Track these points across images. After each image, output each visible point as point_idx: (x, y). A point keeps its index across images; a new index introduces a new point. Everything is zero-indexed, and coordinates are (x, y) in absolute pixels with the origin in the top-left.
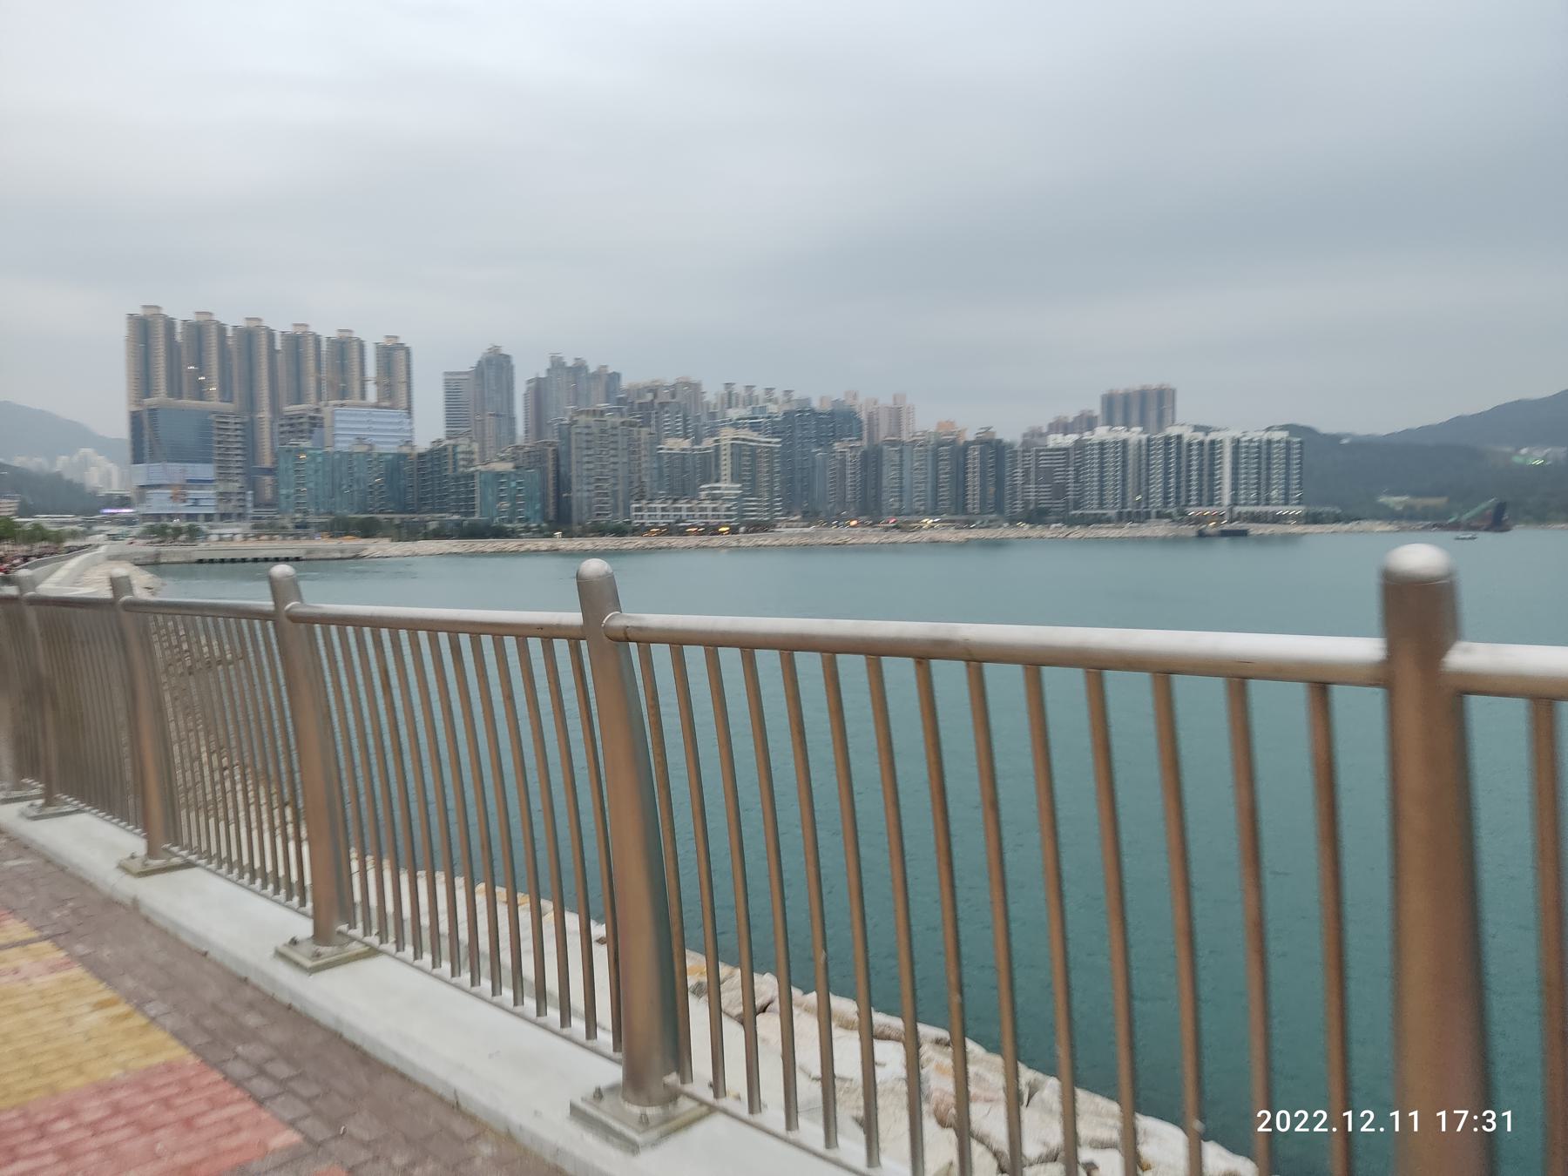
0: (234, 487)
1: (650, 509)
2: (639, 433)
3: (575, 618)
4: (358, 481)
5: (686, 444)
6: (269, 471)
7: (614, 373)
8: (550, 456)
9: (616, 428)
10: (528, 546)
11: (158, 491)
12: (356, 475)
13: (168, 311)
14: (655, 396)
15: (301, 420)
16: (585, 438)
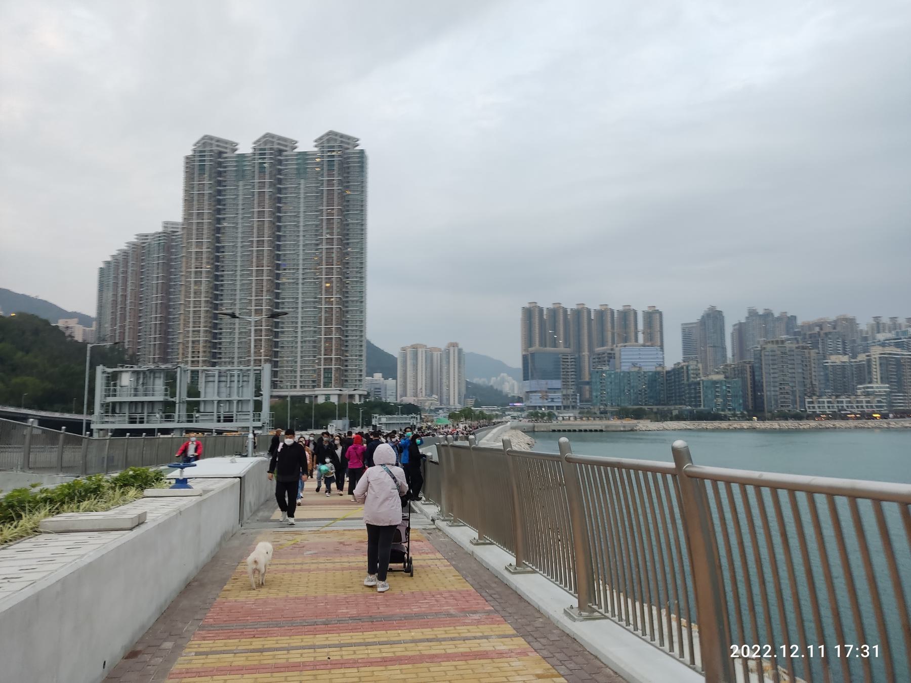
0: (570, 392)
1: (819, 402)
2: (809, 353)
3: (672, 465)
4: (633, 387)
5: (845, 359)
6: (588, 383)
7: (792, 316)
8: (748, 370)
9: (793, 351)
10: (734, 426)
11: (533, 394)
12: (632, 384)
13: (540, 304)
14: (821, 329)
15: (604, 355)
16: (771, 358)
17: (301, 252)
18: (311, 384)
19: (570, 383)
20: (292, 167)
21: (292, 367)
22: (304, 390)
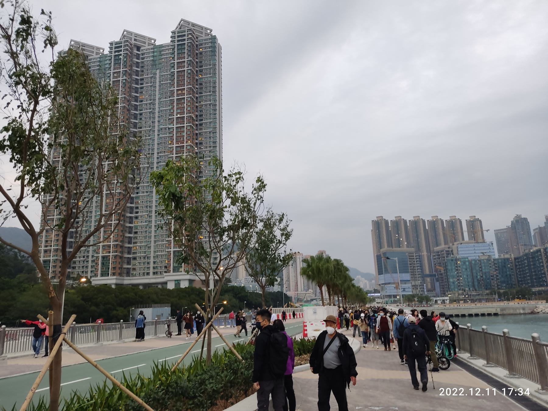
0: (418, 283)
6: (430, 276)
11: (389, 285)
12: (484, 271)
15: (442, 253)
17: (156, 137)
18: (164, 269)
19: (417, 276)
20: (148, 59)
21: (145, 252)
22: (157, 276)
